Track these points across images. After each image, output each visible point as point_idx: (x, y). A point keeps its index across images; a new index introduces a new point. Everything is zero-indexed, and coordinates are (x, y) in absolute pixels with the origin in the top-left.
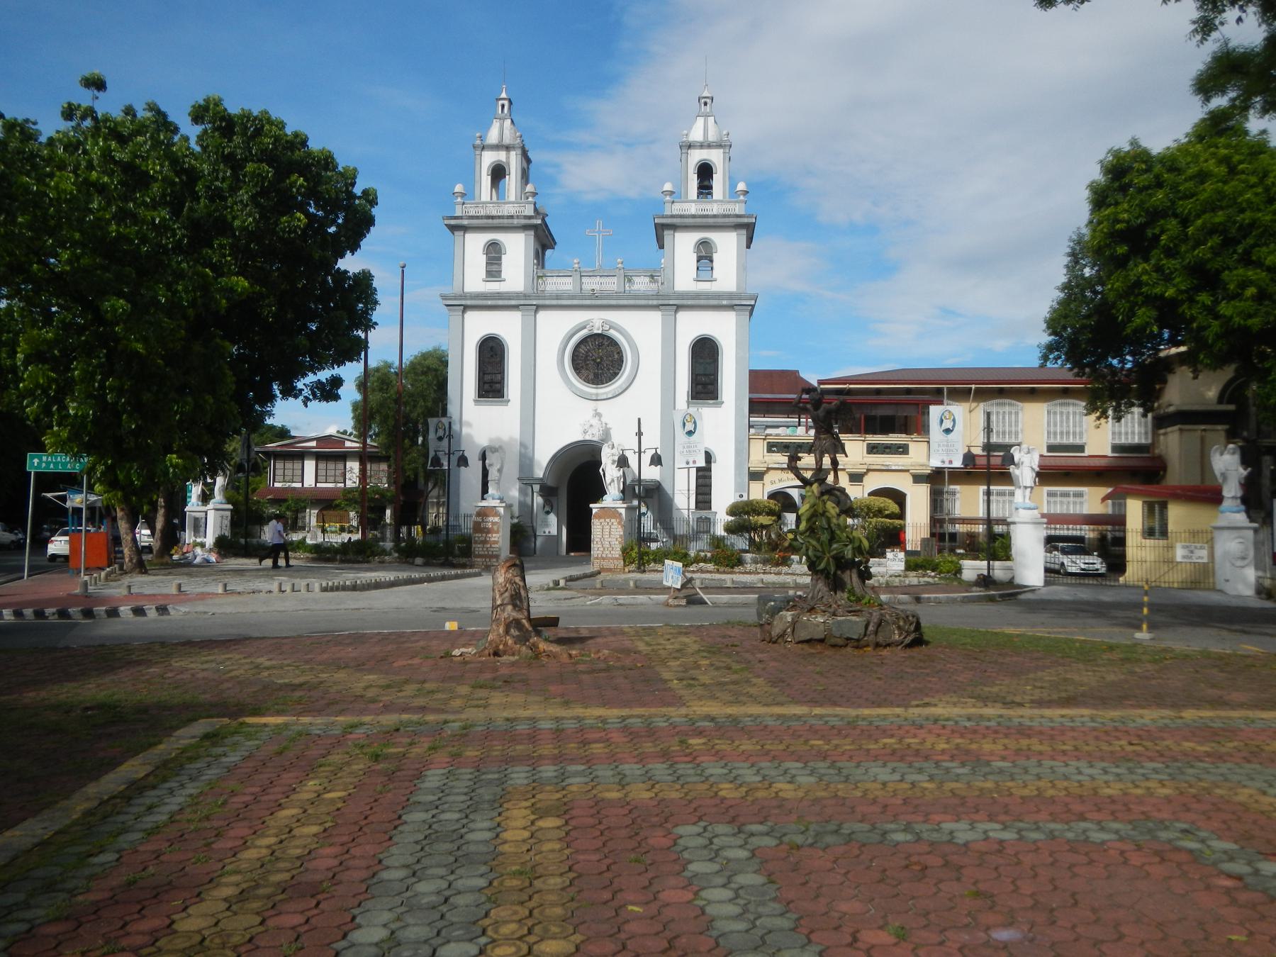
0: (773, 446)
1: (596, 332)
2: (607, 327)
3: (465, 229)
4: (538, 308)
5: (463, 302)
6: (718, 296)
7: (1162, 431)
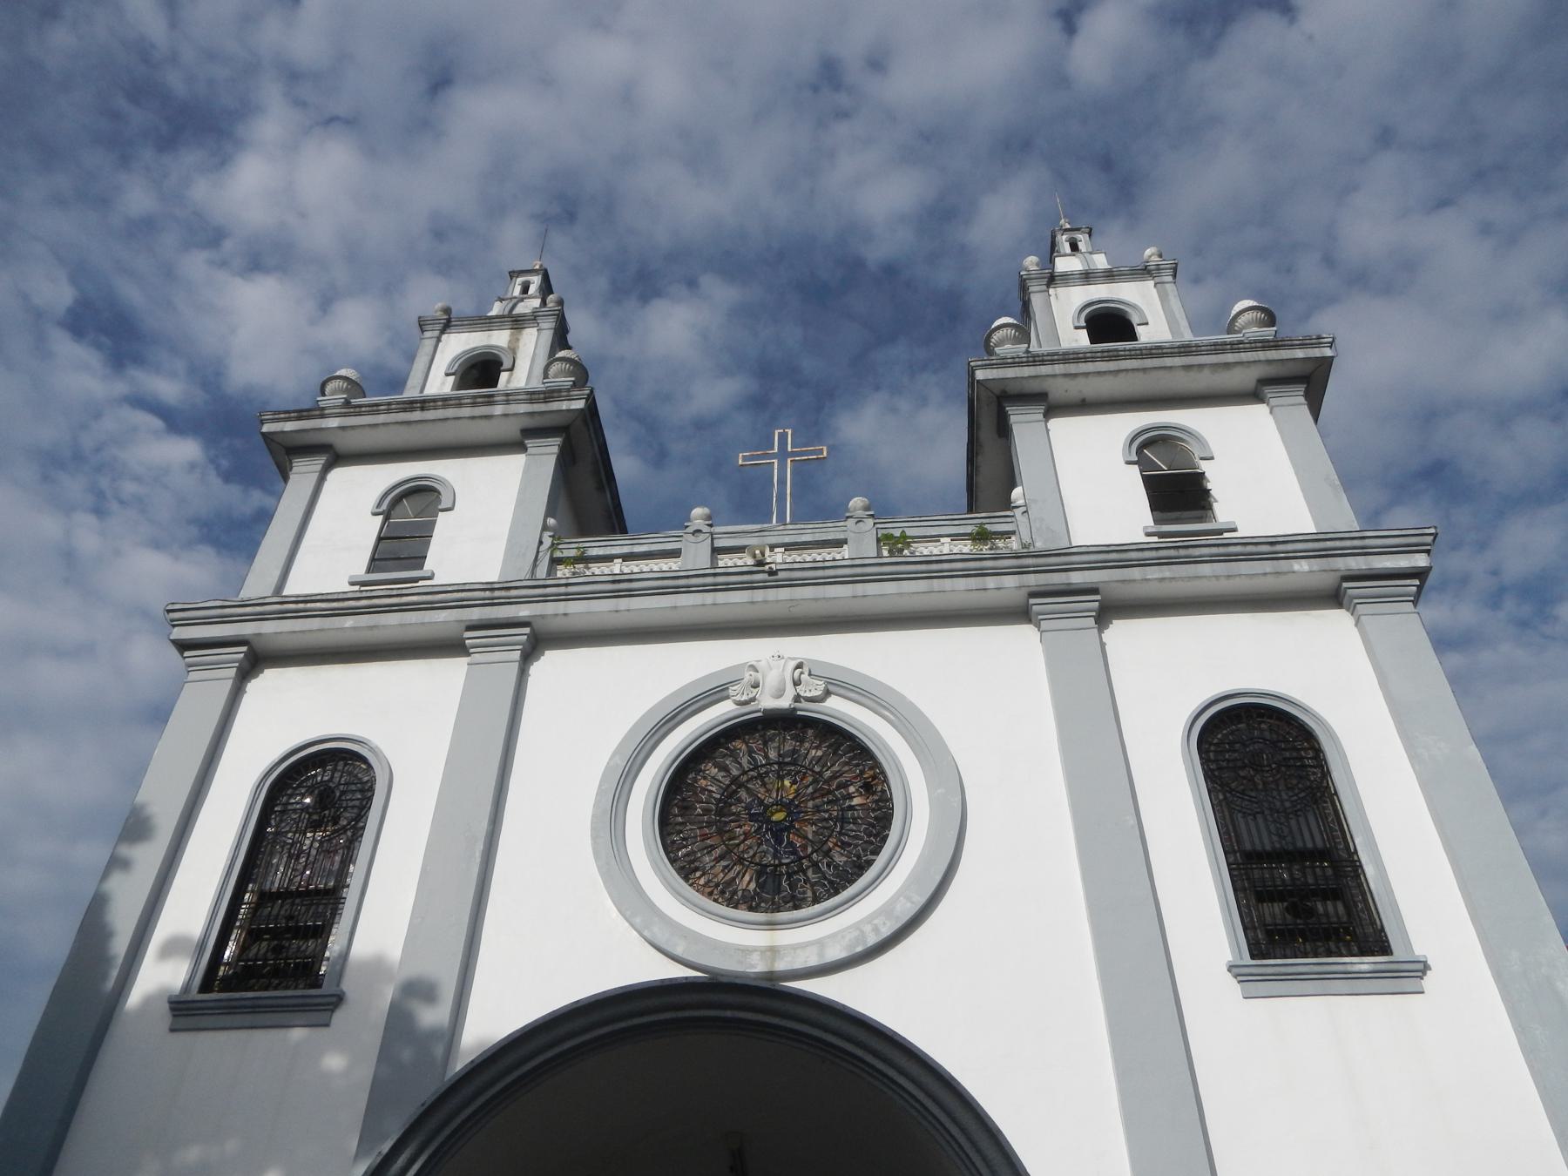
1: (768, 702)
2: (813, 688)
3: (337, 457)
4: (538, 642)
5: (247, 629)
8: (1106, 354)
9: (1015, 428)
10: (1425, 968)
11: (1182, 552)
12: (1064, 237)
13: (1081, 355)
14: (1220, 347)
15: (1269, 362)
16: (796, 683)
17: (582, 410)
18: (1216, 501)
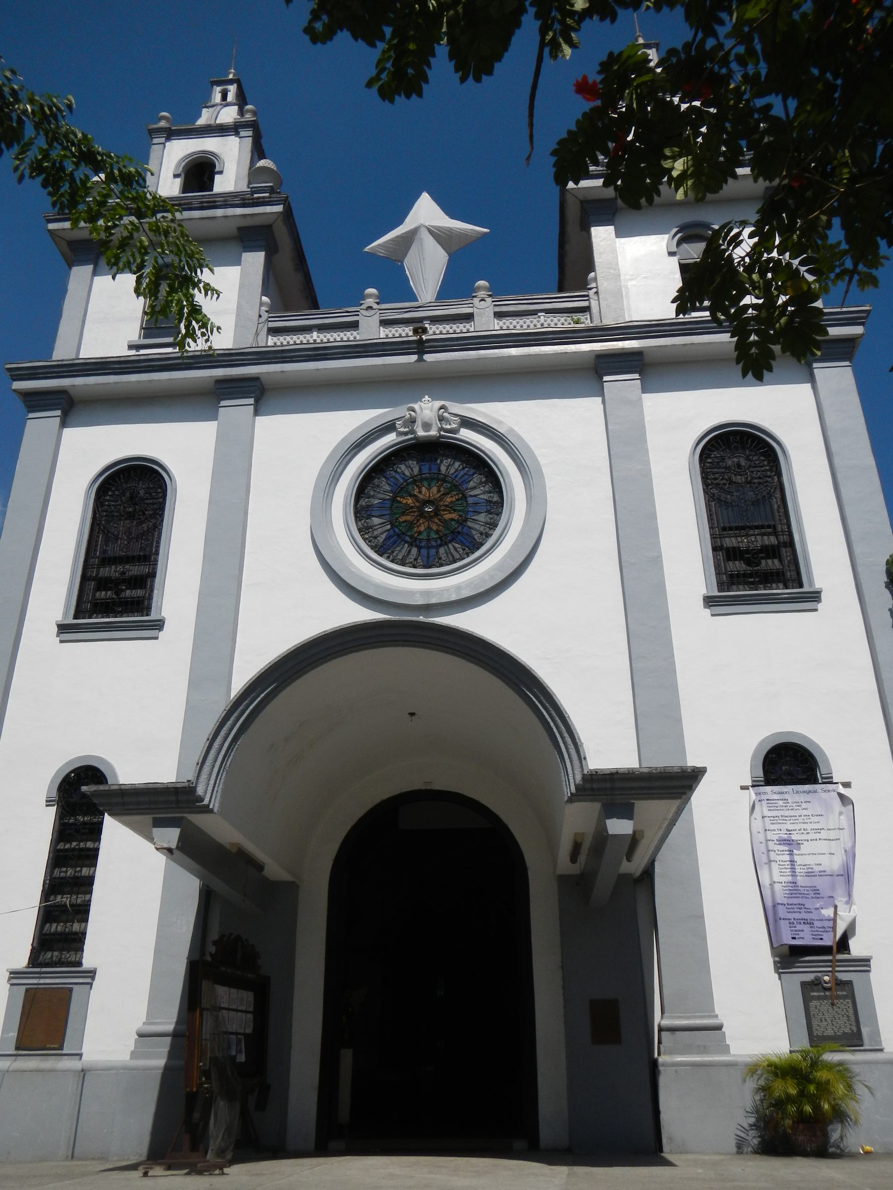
1: (421, 433)
16: (441, 419)
17: (281, 213)
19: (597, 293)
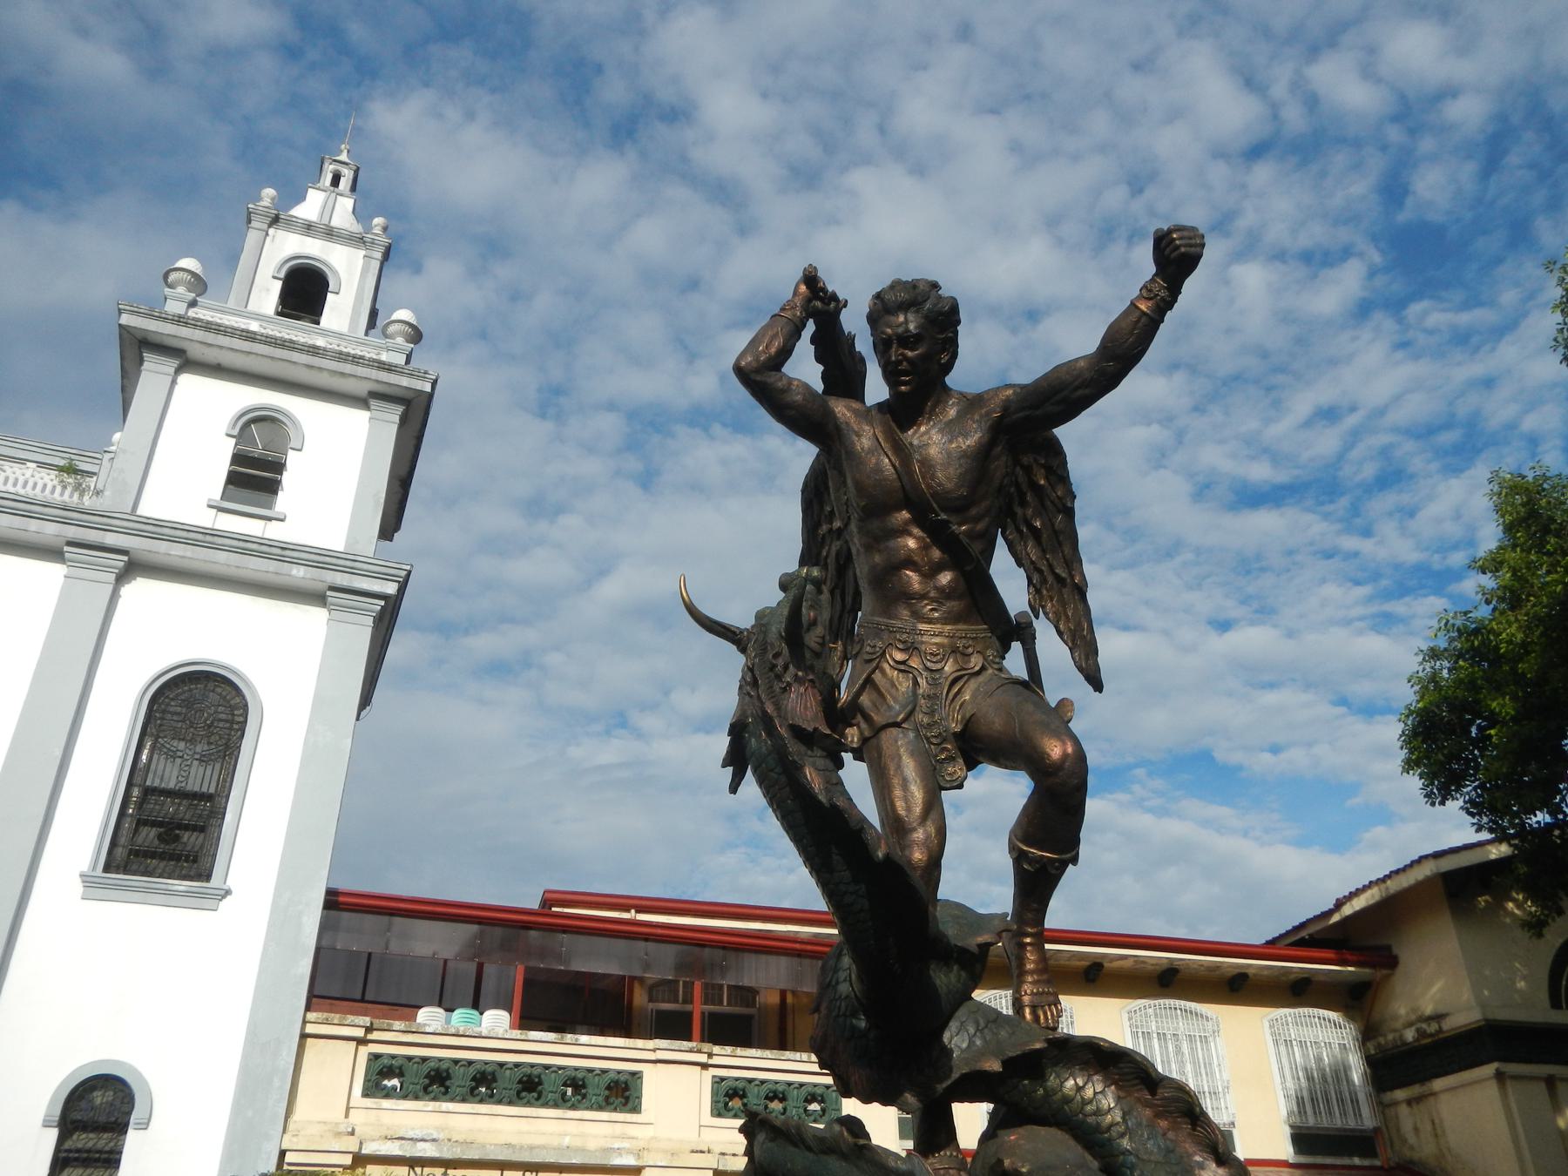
0: (388, 1072)
6: (284, 552)
7: (1400, 1094)
8: (244, 334)
9: (143, 372)
10: (228, 892)
11: (209, 538)
12: (331, 167)
13: (222, 328)
14: (344, 357)
15: (377, 381)
18: (282, 490)
19: (113, 459)
